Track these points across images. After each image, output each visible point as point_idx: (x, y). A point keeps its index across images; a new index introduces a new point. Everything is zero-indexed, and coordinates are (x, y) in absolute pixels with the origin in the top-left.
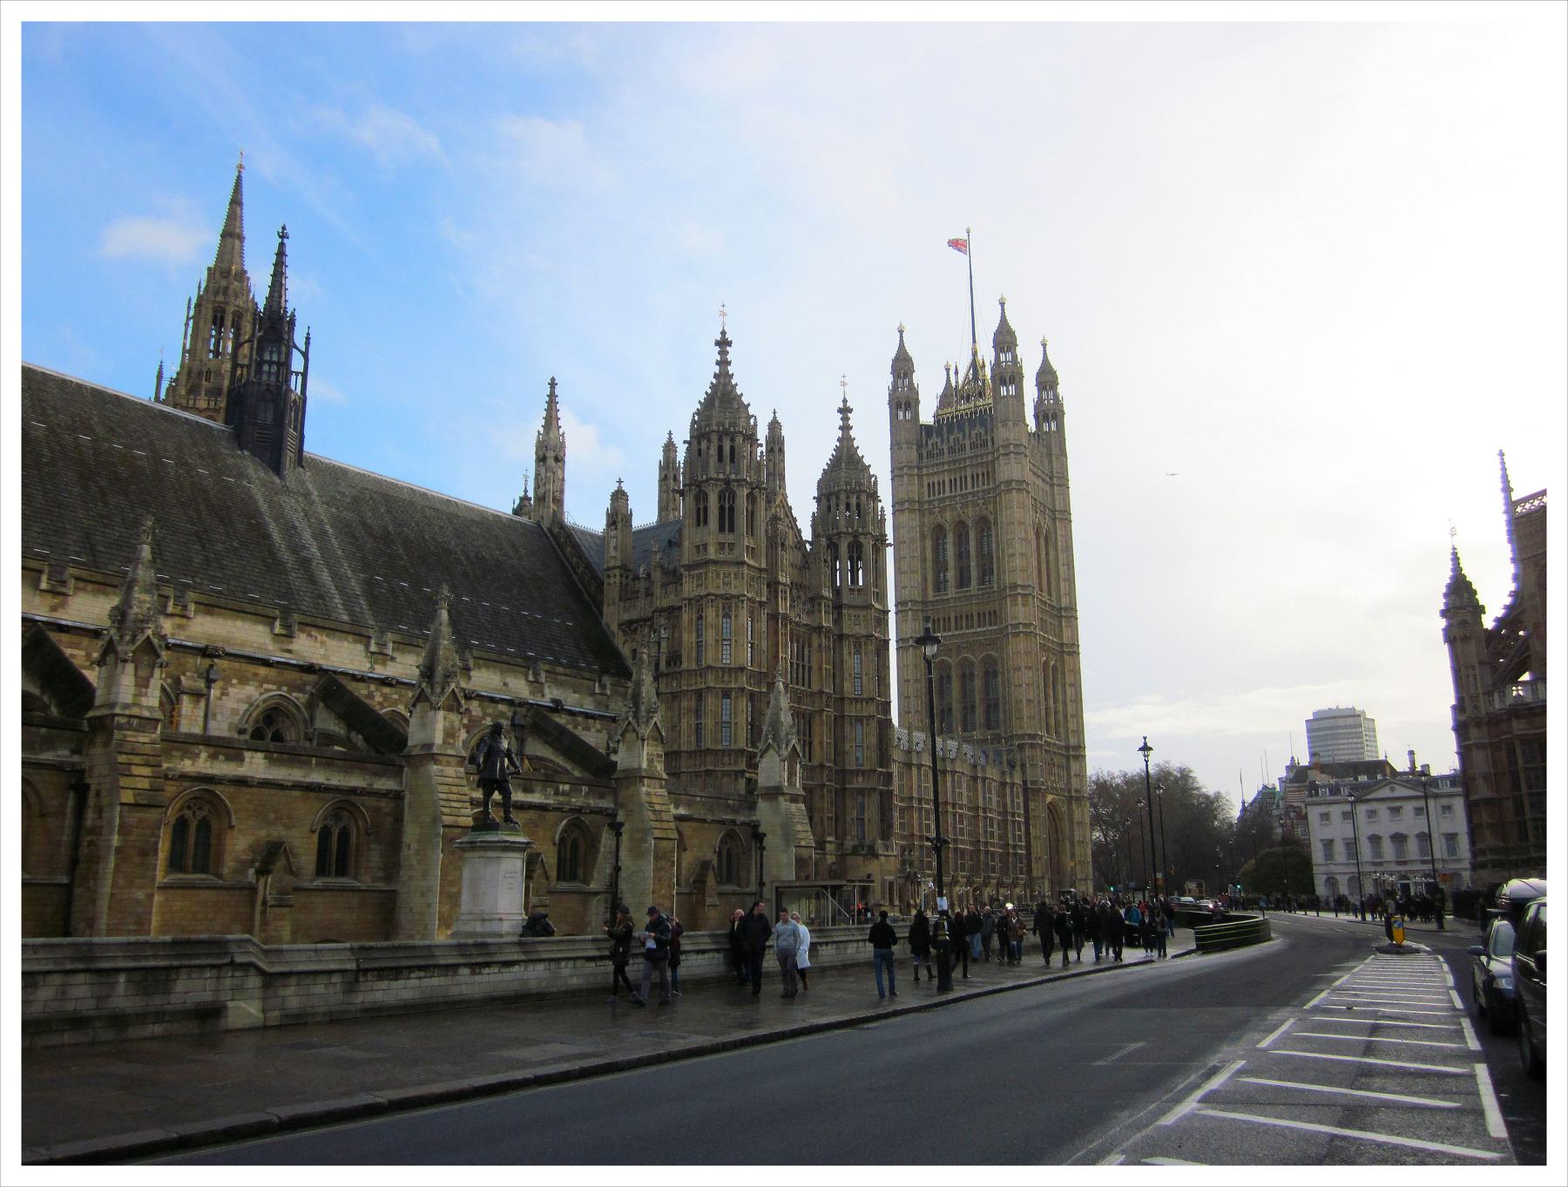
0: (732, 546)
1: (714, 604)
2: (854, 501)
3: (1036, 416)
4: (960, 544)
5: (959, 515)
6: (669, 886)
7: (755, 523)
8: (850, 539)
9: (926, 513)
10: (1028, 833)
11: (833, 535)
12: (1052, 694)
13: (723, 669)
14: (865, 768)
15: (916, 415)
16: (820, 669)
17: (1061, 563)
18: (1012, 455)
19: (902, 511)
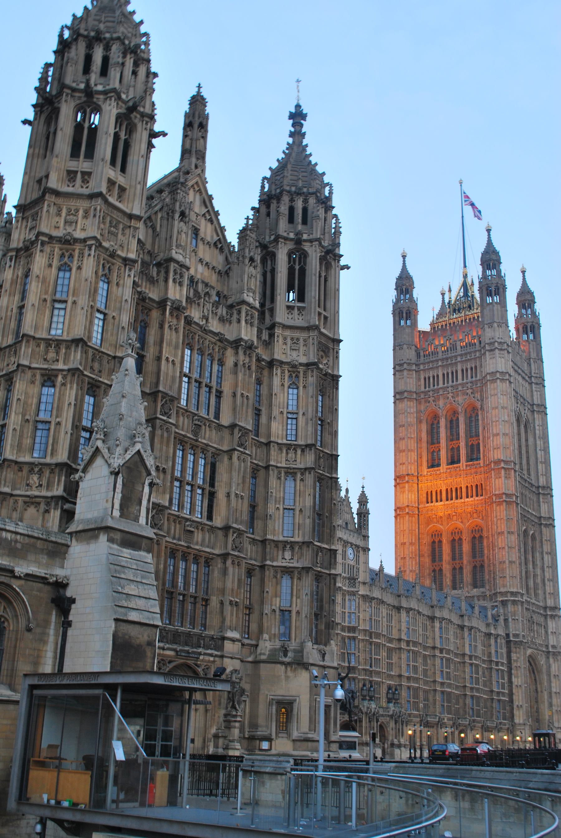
0: (87, 175)
1: (47, 249)
2: (299, 204)
3: (517, 329)
4: (451, 428)
5: (451, 403)
7: (130, 159)
8: (291, 246)
9: (423, 400)
10: (510, 682)
11: (270, 242)
12: (531, 559)
14: (296, 539)
15: (415, 324)
16: (234, 395)
17: (538, 448)
18: (497, 350)
19: (401, 400)
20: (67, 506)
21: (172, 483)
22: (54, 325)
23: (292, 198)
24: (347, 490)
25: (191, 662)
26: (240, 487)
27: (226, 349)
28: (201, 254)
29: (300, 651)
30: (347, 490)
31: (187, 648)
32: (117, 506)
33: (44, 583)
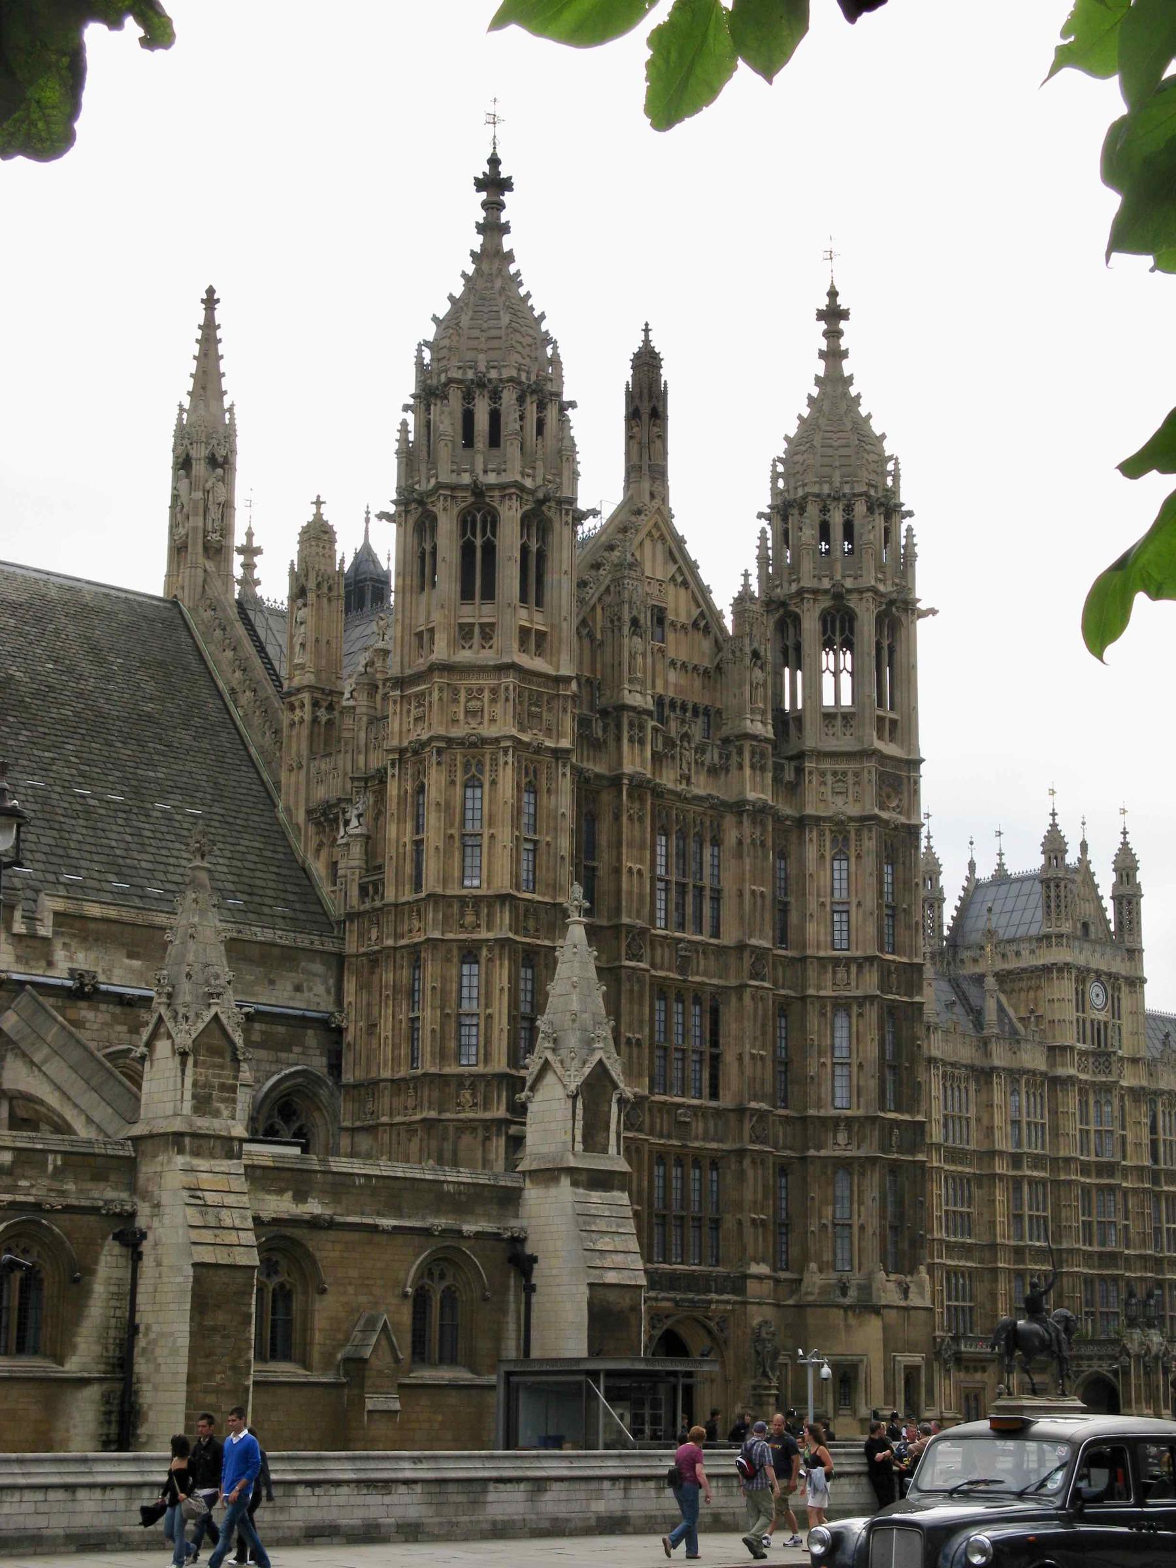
1: (445, 758)
2: (837, 518)
6: (234, 1368)
7: (548, 578)
8: (826, 603)
11: (791, 596)
13: (462, 899)
16: (741, 894)
20: (513, 1130)
21: (651, 1053)
22: (468, 872)
23: (825, 507)
24: (1084, 846)
25: (698, 1314)
26: (758, 1043)
27: (722, 817)
28: (671, 654)
29: (866, 1289)
30: (1084, 846)
31: (691, 1296)
32: (579, 1138)
33: (497, 1240)
